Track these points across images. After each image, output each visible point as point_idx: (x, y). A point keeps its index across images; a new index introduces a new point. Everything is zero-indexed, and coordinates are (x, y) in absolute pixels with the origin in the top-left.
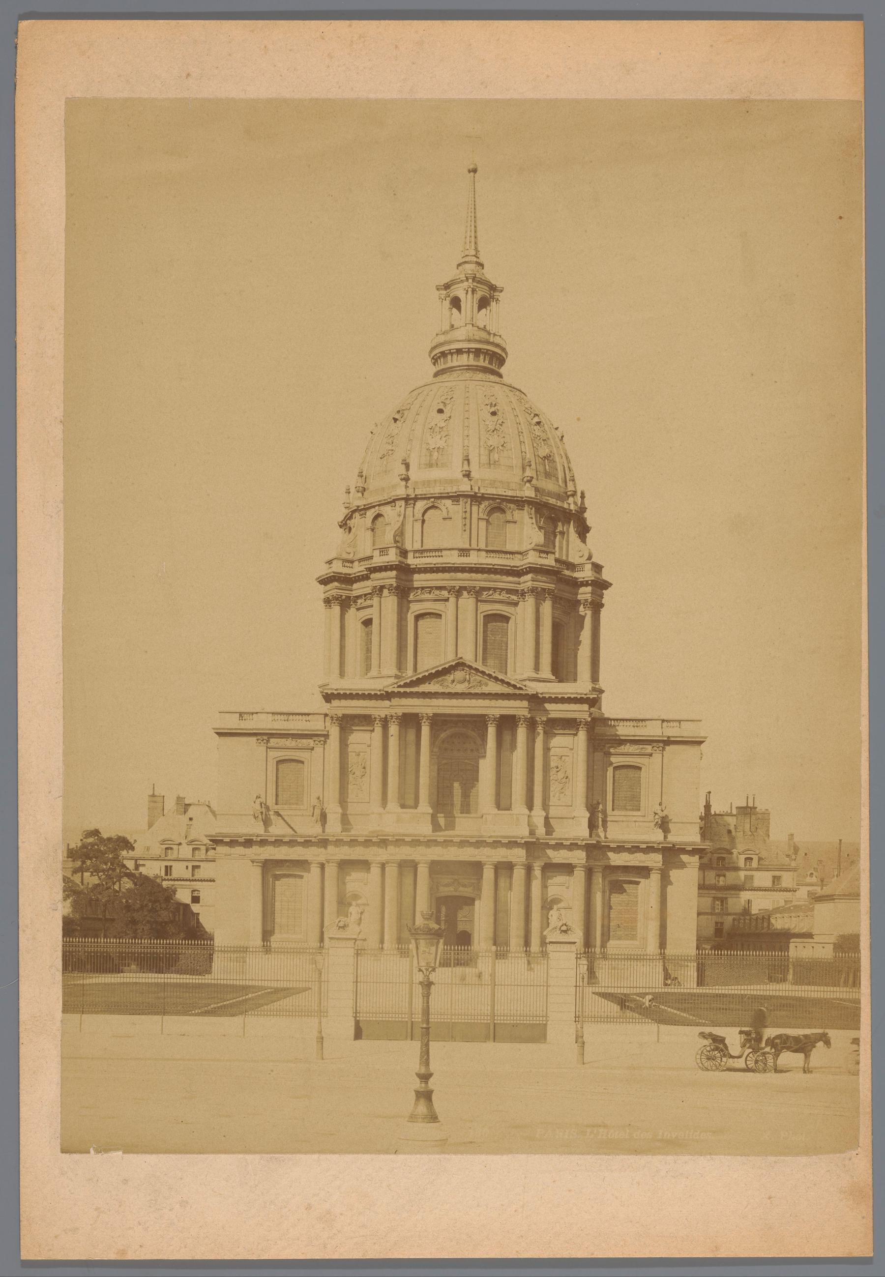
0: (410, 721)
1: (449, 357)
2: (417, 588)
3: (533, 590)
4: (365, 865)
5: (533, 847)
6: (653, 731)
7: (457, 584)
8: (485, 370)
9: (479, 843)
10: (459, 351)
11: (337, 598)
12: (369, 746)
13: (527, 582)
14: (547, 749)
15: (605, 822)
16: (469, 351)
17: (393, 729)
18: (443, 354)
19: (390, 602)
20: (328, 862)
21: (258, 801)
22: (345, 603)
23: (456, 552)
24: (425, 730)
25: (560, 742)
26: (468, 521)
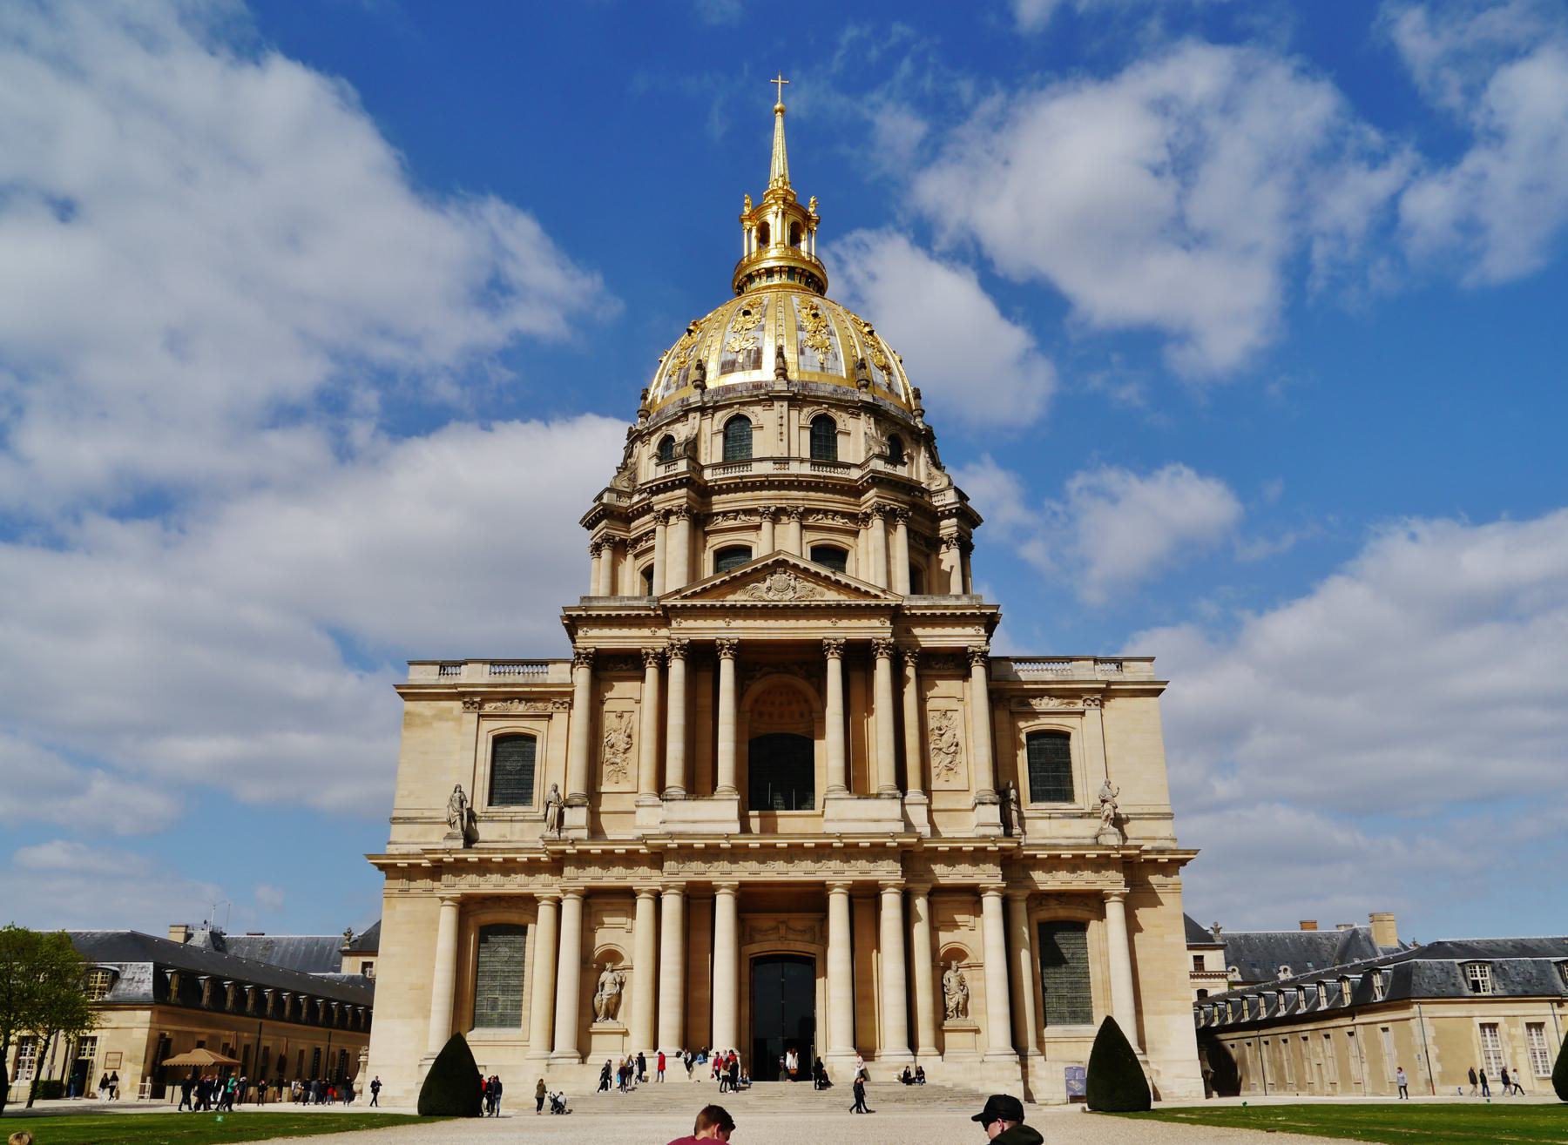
2: (718, 514)
3: (879, 509)
5: (914, 858)
6: (1084, 673)
9: (822, 852)
10: (770, 272)
11: (608, 539)
12: (638, 702)
14: (922, 701)
15: (1021, 818)
16: (781, 270)
19: (679, 530)
20: (565, 892)
22: (620, 548)
23: (770, 464)
24: (727, 668)
25: (944, 687)
26: (785, 429)
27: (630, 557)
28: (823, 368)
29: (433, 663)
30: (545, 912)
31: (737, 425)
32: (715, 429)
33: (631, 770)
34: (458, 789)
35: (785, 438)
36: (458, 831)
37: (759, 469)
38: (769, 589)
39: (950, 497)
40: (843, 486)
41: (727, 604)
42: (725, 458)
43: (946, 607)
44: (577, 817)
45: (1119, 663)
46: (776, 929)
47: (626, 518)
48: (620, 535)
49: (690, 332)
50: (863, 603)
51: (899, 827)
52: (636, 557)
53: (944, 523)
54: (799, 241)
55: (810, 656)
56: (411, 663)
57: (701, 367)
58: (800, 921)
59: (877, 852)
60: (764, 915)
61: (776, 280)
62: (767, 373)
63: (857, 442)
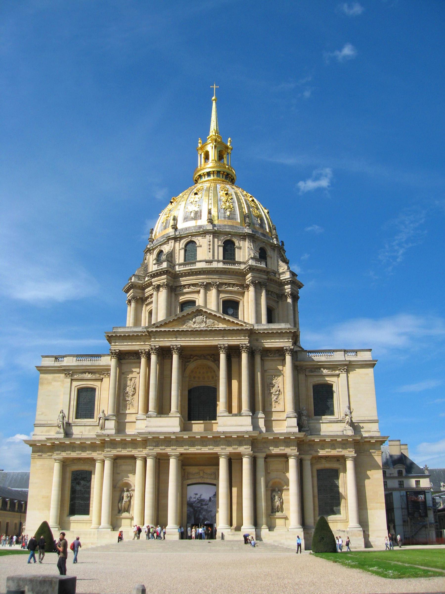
0: (164, 353)
1: (203, 177)
3: (253, 282)
4: (134, 458)
6: (339, 357)
7: (206, 281)
8: (223, 181)
10: (209, 174)
11: (133, 298)
13: (249, 277)
17: (153, 358)
18: (200, 176)
19: (163, 294)
21: (61, 414)
23: (204, 263)
24: (175, 357)
26: (211, 247)
27: (144, 306)
28: (229, 218)
29: (52, 356)
30: (98, 465)
31: (190, 245)
32: (181, 247)
33: (135, 404)
34: (62, 412)
35: (211, 251)
36: (62, 430)
37: (199, 266)
38: (195, 323)
39: (287, 276)
40: (237, 272)
41: (176, 329)
42: (185, 260)
43: (275, 329)
44: (111, 425)
45: (356, 351)
46: (198, 473)
47: (143, 288)
48: (141, 295)
49: (171, 202)
50: (235, 328)
51: (250, 429)
52: (147, 305)
53: (286, 287)
54: (223, 158)
55: (212, 353)
56: (43, 357)
57: (175, 219)
58: (209, 470)
59: (240, 440)
60: (194, 467)
61: (212, 177)
62: (203, 221)
63: (245, 252)
